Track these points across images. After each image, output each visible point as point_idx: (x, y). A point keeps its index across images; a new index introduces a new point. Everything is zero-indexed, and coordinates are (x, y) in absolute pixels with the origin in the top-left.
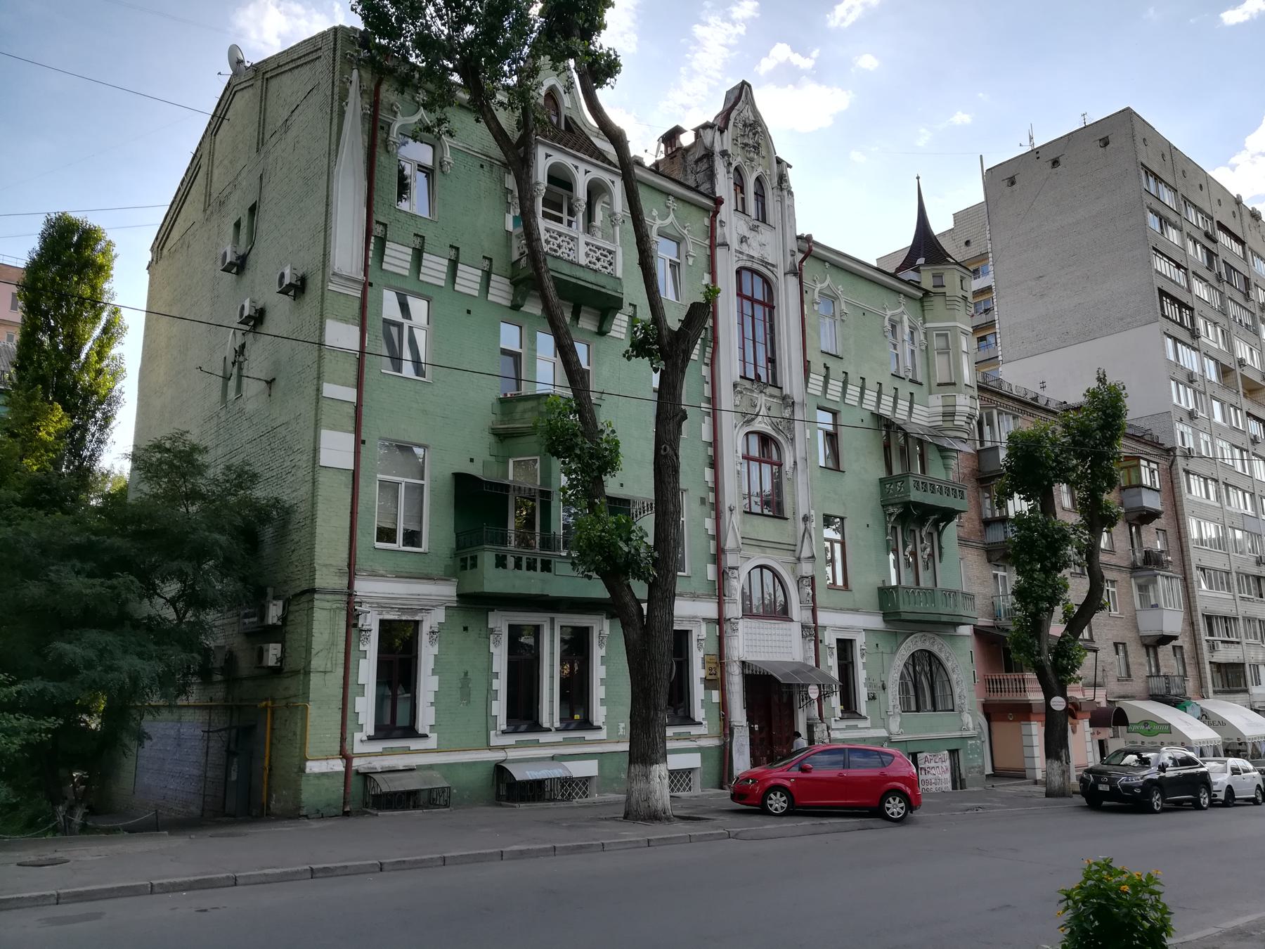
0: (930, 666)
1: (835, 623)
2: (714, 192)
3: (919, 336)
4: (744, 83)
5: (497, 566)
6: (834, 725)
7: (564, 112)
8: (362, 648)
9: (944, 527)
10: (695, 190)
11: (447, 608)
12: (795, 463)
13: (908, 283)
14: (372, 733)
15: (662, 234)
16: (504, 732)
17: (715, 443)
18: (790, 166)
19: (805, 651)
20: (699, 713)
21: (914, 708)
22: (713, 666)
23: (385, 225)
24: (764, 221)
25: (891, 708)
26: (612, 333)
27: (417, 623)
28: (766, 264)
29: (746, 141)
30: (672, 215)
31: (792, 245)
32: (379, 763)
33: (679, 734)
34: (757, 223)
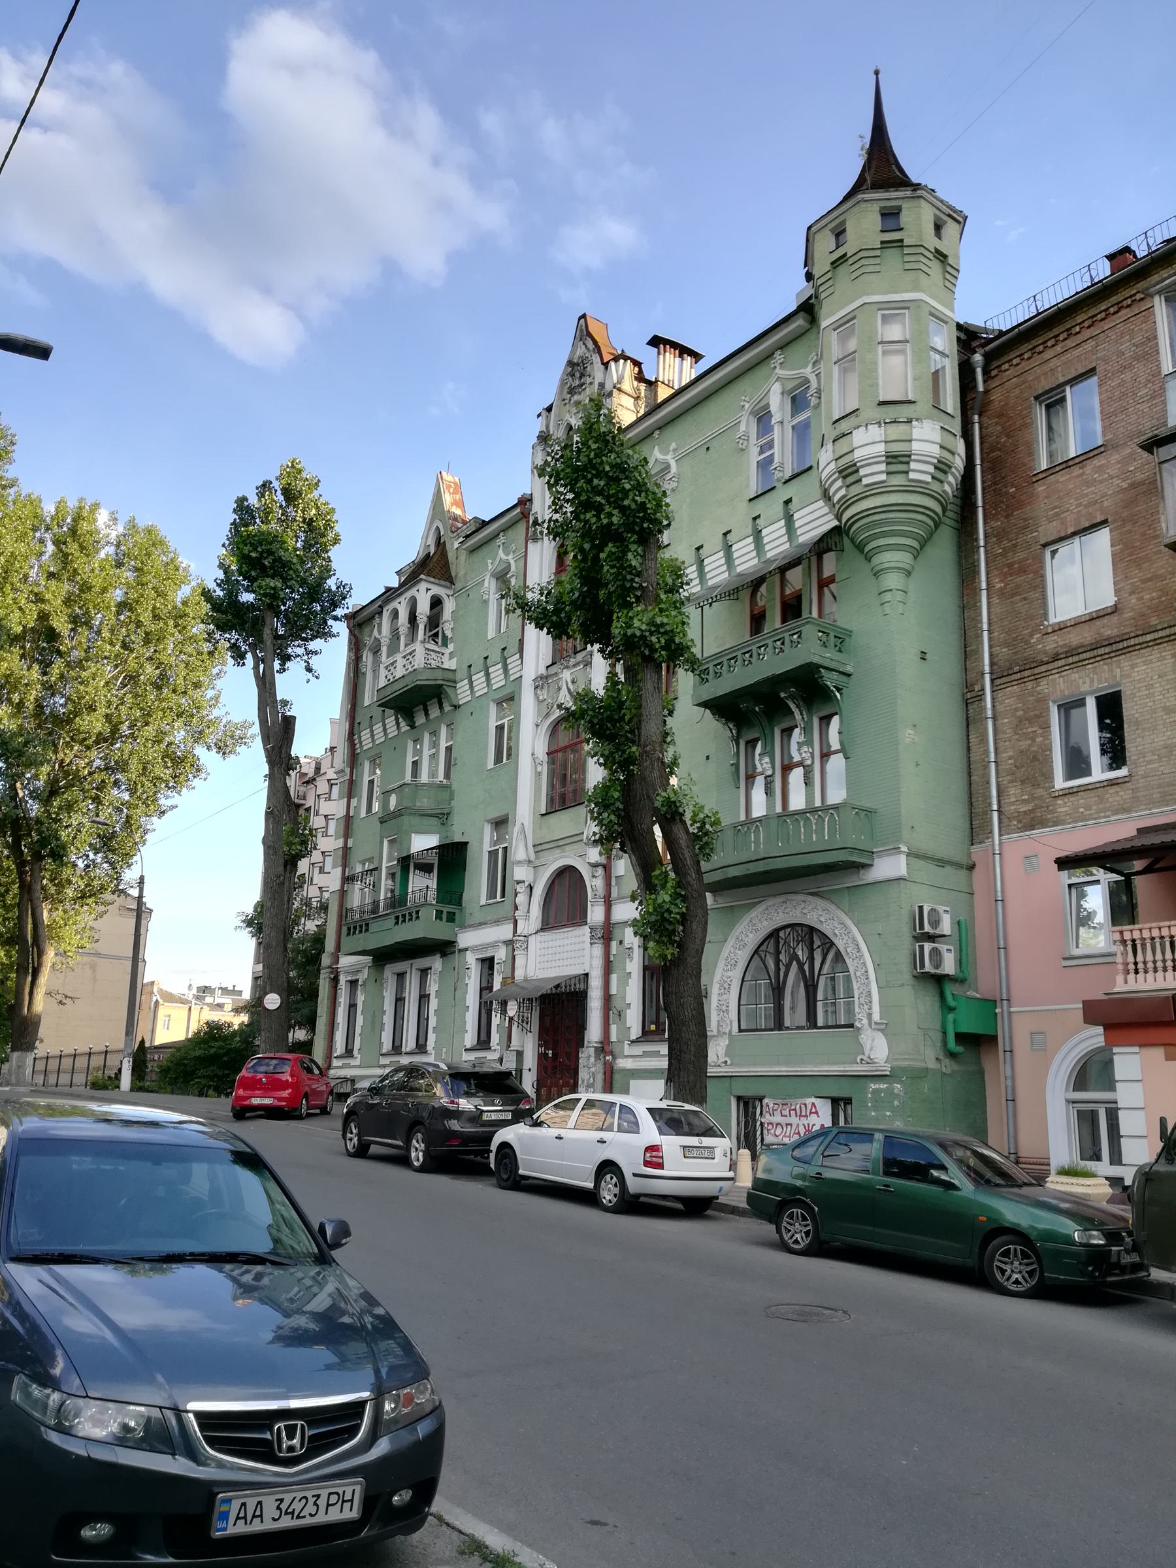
6: (627, 1050)
30: (501, 551)
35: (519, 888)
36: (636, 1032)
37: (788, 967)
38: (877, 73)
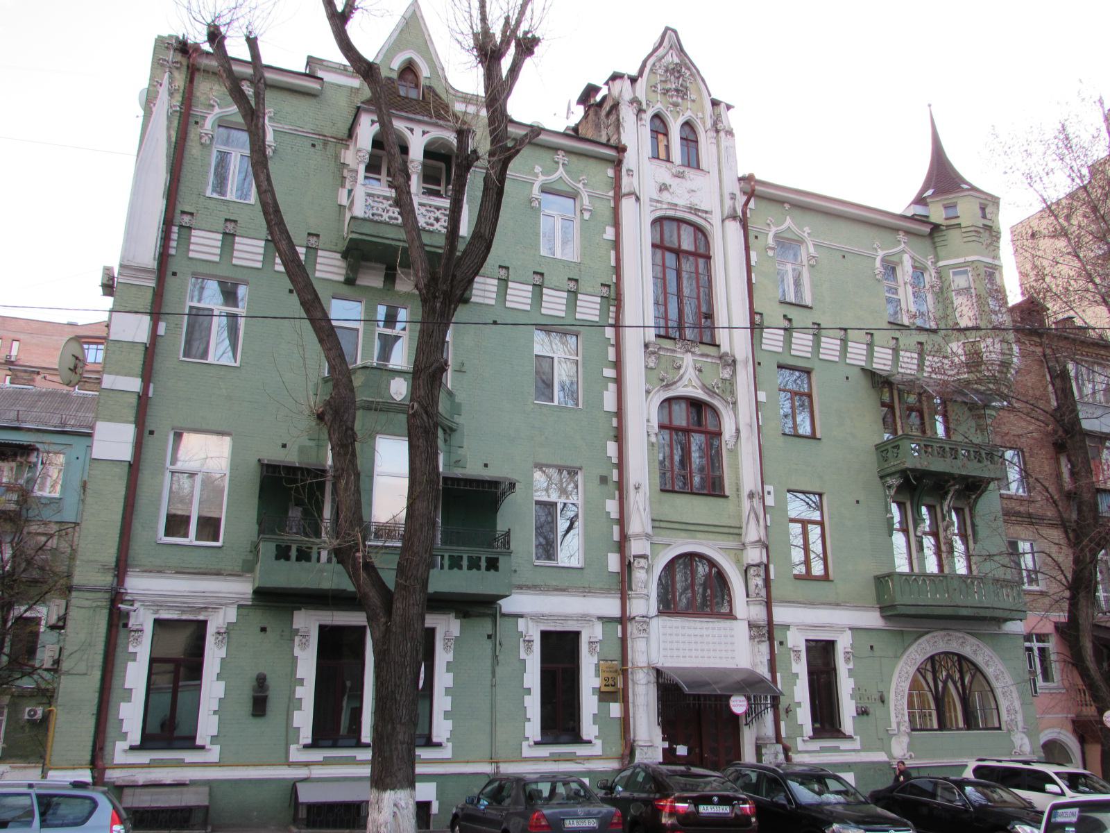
0: (961, 672)
1: (801, 622)
2: (620, 141)
3: (930, 278)
4: (667, 29)
5: (278, 558)
6: (800, 745)
7: (423, 82)
8: (131, 649)
9: (976, 501)
10: (607, 145)
11: (240, 607)
12: (738, 431)
13: (913, 218)
14: (138, 742)
15: (545, 190)
16: (306, 747)
17: (620, 413)
18: (729, 107)
19: (754, 655)
20: (589, 729)
21: (935, 726)
22: (610, 675)
23: (192, 214)
24: (698, 167)
25: (894, 726)
26: (473, 299)
27: (205, 623)
28: (695, 210)
29: (668, 86)
30: (561, 169)
31: (733, 186)
32: (142, 777)
33: (560, 754)
34: (681, 169)
35: (643, 562)
36: (808, 729)
37: (945, 683)
38: (930, 106)
